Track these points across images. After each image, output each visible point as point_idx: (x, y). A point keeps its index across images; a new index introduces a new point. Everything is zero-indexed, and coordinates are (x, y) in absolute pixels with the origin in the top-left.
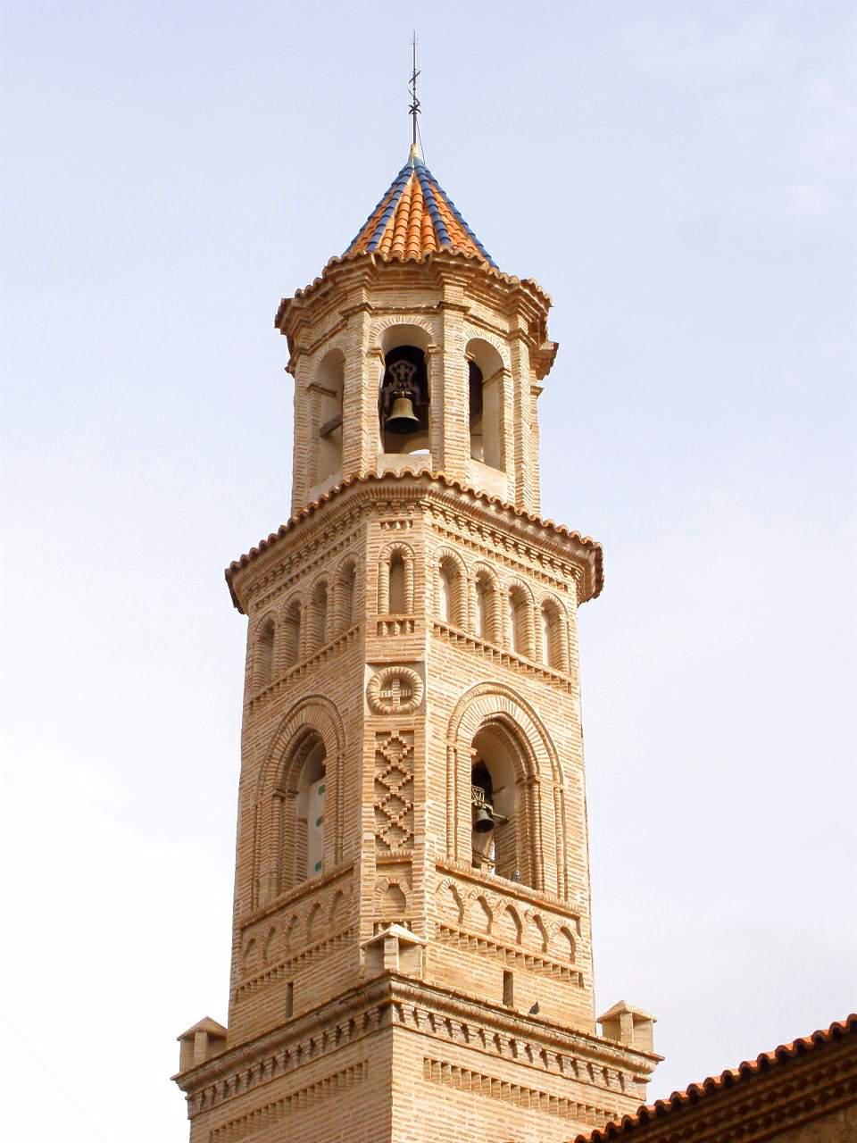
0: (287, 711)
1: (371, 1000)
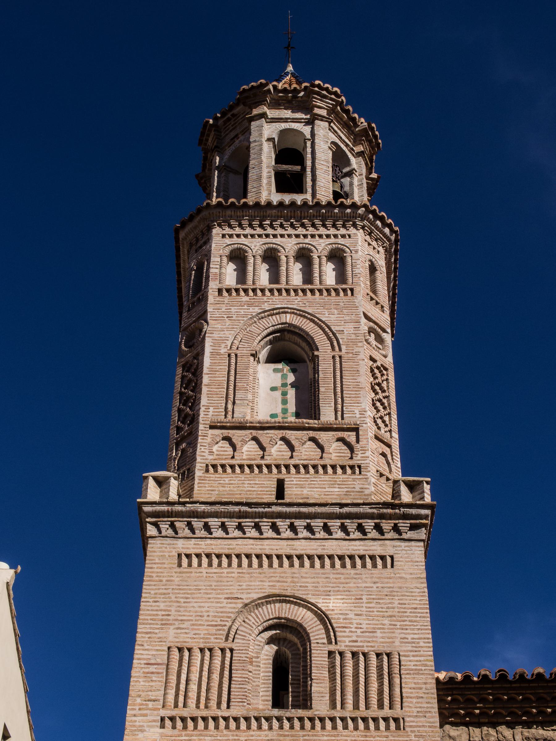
0: (267, 309)
1: (405, 517)
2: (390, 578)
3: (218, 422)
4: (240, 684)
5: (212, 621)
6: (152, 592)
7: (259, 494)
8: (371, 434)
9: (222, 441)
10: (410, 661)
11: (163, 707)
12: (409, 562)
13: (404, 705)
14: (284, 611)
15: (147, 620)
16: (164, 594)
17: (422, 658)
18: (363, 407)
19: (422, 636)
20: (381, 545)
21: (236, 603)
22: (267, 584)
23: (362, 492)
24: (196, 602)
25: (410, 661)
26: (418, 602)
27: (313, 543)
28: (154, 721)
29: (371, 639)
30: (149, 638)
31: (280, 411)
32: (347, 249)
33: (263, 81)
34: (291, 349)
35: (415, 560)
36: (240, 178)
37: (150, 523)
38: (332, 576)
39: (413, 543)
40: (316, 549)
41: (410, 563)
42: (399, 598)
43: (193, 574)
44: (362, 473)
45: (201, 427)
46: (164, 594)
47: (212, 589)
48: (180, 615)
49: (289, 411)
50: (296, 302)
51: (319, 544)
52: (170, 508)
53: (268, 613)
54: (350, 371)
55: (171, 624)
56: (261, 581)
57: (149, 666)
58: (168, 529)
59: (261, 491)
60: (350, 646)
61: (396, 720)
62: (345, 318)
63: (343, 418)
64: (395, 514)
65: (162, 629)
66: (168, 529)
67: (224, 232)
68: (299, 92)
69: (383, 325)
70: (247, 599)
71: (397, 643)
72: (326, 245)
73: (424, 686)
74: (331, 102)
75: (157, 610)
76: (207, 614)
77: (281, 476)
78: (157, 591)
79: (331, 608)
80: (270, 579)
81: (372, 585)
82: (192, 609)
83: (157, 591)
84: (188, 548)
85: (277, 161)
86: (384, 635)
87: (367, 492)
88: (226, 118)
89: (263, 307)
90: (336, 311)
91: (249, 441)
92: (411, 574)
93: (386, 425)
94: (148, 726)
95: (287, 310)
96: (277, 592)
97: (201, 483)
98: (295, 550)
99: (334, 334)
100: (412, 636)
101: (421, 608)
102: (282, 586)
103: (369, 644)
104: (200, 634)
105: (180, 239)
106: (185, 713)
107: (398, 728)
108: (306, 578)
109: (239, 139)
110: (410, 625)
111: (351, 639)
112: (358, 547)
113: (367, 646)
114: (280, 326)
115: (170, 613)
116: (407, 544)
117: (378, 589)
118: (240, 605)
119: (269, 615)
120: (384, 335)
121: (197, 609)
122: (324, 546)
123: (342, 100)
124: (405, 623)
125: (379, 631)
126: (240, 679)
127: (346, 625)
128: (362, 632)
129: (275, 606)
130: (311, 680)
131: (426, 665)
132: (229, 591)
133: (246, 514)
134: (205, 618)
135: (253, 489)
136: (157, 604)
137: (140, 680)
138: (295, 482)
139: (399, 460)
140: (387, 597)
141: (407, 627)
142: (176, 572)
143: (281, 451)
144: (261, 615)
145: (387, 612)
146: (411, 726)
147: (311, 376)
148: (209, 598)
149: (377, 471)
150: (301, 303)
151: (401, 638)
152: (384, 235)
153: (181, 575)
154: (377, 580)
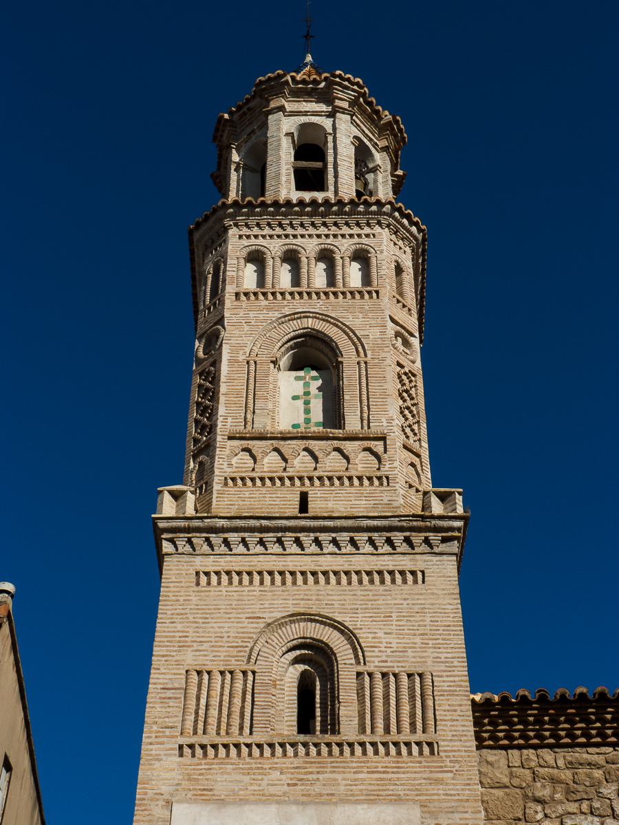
0: (287, 313)
1: (436, 530)
2: (421, 594)
3: (237, 433)
4: (263, 709)
5: (233, 642)
6: (169, 612)
7: (281, 508)
8: (399, 444)
9: (241, 453)
10: (444, 682)
11: (182, 734)
12: (441, 577)
13: (437, 728)
14: (309, 631)
15: (164, 642)
16: (182, 614)
17: (456, 679)
18: (390, 415)
19: (456, 655)
20: (411, 560)
21: (258, 623)
22: (291, 602)
23: (390, 504)
24: (215, 622)
25: (444, 682)
26: (451, 619)
27: (339, 558)
28: (172, 749)
29: (402, 659)
30: (166, 661)
31: (303, 421)
32: (372, 249)
33: (280, 72)
34: (314, 353)
35: (447, 575)
36: (258, 175)
37: (166, 539)
38: (359, 593)
39: (445, 557)
40: (343, 565)
41: (443, 579)
42: (431, 615)
43: (212, 593)
44: (390, 484)
45: (219, 438)
46: (182, 614)
47: (233, 609)
48: (199, 637)
49: (312, 421)
50: (318, 305)
51: (345, 559)
52: (187, 524)
53: (292, 633)
54: (376, 377)
55: (189, 646)
56: (285, 599)
57: (166, 691)
58: (185, 546)
59: (283, 505)
60: (379, 667)
61: (430, 744)
62: (370, 322)
63: (369, 427)
64: (426, 527)
66: (185, 546)
67: (241, 233)
68: (319, 83)
69: (410, 329)
70: (270, 618)
71: (430, 663)
72: (349, 246)
73: (458, 708)
74: (353, 93)
75: (174, 632)
76: (228, 634)
77: (304, 489)
78: (173, 612)
79: (359, 626)
80: (294, 597)
81: (402, 602)
82: (211, 630)
83: (173, 612)
84: (206, 566)
85: (296, 158)
86: (416, 654)
87: (395, 504)
88: (241, 112)
89: (283, 312)
90: (361, 315)
91: (270, 452)
92: (443, 590)
93: (415, 434)
94: (165, 755)
95: (308, 314)
96: (302, 610)
97: (220, 497)
98: (320, 566)
99: (359, 339)
100: (446, 655)
101: (454, 626)
102: (307, 604)
103: (400, 664)
104: (220, 656)
105: (195, 241)
106: (205, 740)
107: (432, 753)
108: (332, 595)
109: (256, 135)
110: (443, 644)
111: (380, 659)
112: (387, 563)
113: (398, 667)
114: (302, 331)
115: (188, 635)
116: (438, 558)
117: (408, 606)
118: (262, 625)
119: (293, 635)
120: (412, 340)
121: (217, 630)
122: (351, 561)
123: (365, 91)
124: (437, 642)
125: (410, 650)
126: (263, 704)
127: (376, 645)
128: (393, 652)
129: (299, 626)
130: (339, 702)
131: (461, 686)
132: (251, 610)
133: (265, 529)
134: (225, 639)
135: (275, 503)
136: (175, 625)
137: (157, 706)
138: (319, 495)
139: (429, 471)
140: (418, 615)
141: (440, 646)
142: (194, 591)
143: (303, 463)
144: (284, 635)
145: (418, 630)
146: (445, 751)
147: (335, 383)
148: (230, 618)
149: (406, 482)
150: (323, 307)
151: (434, 658)
152: (411, 234)
153: (199, 594)
154: (407, 597)
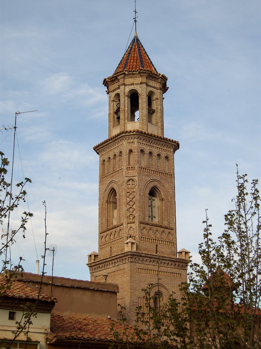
6: (133, 280)
16: (135, 281)
65: (135, 292)
81: (177, 282)
